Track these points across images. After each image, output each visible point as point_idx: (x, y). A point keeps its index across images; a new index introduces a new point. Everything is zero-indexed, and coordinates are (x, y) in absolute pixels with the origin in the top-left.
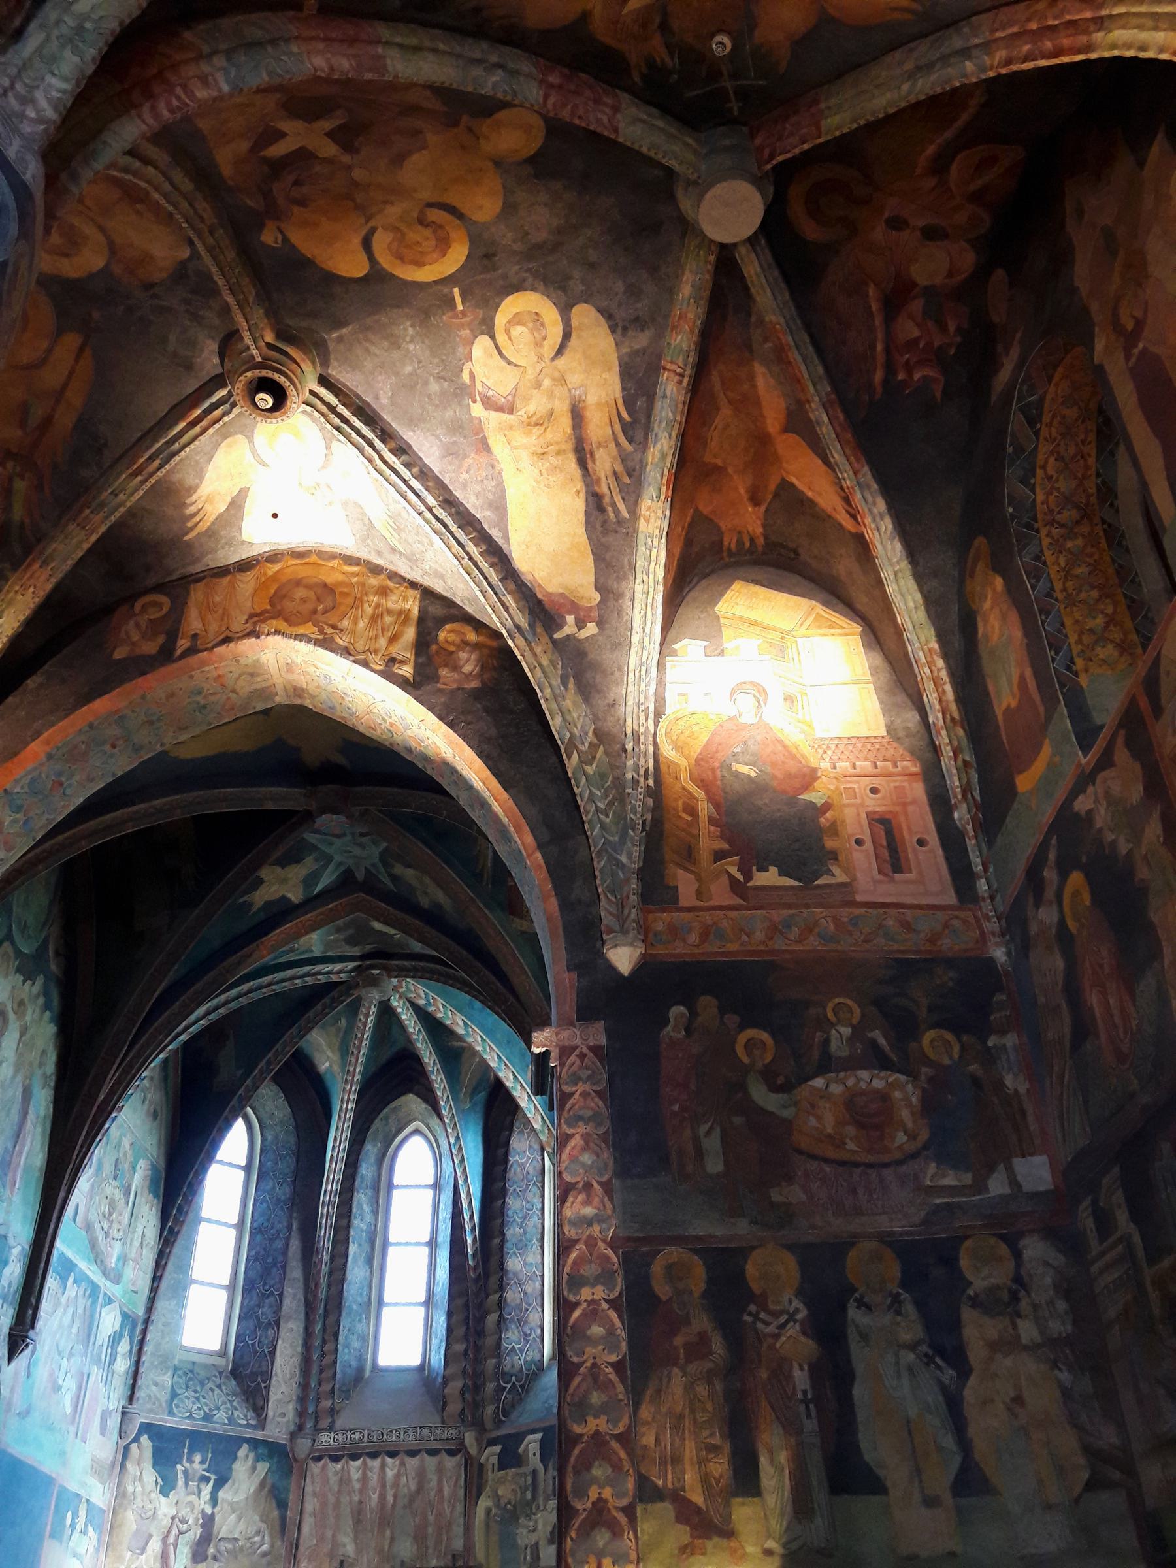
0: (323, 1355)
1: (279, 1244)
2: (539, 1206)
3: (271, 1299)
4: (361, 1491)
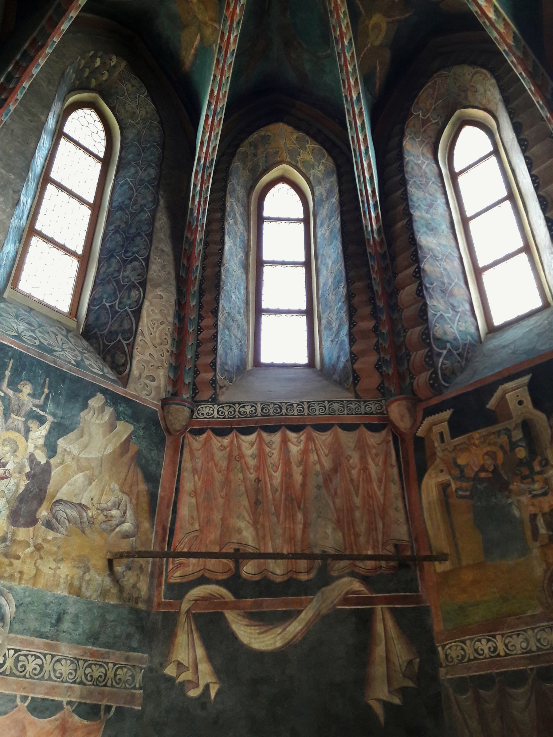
0: (199, 330)
1: (145, 216)
2: (444, 201)
3: (135, 263)
4: (258, 468)
